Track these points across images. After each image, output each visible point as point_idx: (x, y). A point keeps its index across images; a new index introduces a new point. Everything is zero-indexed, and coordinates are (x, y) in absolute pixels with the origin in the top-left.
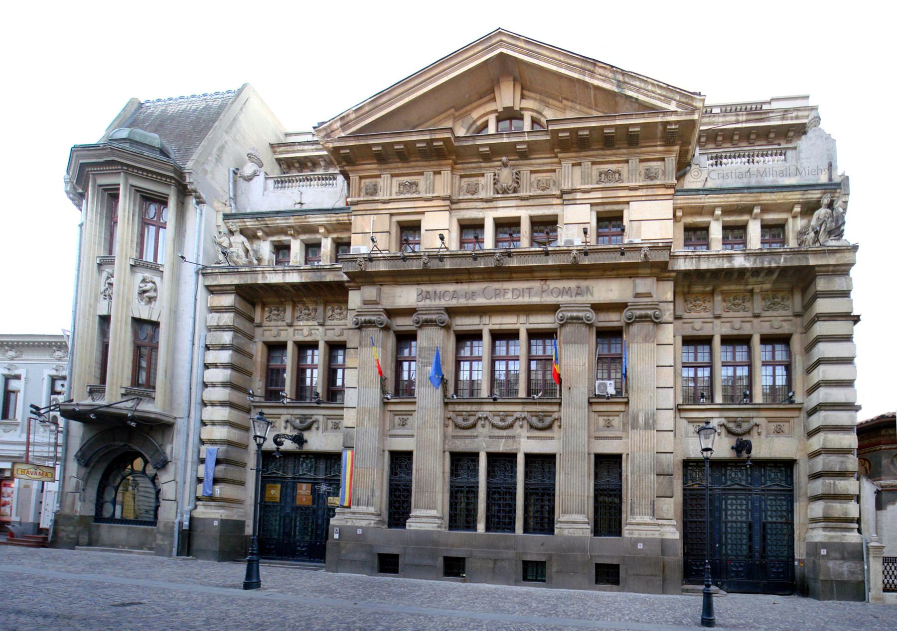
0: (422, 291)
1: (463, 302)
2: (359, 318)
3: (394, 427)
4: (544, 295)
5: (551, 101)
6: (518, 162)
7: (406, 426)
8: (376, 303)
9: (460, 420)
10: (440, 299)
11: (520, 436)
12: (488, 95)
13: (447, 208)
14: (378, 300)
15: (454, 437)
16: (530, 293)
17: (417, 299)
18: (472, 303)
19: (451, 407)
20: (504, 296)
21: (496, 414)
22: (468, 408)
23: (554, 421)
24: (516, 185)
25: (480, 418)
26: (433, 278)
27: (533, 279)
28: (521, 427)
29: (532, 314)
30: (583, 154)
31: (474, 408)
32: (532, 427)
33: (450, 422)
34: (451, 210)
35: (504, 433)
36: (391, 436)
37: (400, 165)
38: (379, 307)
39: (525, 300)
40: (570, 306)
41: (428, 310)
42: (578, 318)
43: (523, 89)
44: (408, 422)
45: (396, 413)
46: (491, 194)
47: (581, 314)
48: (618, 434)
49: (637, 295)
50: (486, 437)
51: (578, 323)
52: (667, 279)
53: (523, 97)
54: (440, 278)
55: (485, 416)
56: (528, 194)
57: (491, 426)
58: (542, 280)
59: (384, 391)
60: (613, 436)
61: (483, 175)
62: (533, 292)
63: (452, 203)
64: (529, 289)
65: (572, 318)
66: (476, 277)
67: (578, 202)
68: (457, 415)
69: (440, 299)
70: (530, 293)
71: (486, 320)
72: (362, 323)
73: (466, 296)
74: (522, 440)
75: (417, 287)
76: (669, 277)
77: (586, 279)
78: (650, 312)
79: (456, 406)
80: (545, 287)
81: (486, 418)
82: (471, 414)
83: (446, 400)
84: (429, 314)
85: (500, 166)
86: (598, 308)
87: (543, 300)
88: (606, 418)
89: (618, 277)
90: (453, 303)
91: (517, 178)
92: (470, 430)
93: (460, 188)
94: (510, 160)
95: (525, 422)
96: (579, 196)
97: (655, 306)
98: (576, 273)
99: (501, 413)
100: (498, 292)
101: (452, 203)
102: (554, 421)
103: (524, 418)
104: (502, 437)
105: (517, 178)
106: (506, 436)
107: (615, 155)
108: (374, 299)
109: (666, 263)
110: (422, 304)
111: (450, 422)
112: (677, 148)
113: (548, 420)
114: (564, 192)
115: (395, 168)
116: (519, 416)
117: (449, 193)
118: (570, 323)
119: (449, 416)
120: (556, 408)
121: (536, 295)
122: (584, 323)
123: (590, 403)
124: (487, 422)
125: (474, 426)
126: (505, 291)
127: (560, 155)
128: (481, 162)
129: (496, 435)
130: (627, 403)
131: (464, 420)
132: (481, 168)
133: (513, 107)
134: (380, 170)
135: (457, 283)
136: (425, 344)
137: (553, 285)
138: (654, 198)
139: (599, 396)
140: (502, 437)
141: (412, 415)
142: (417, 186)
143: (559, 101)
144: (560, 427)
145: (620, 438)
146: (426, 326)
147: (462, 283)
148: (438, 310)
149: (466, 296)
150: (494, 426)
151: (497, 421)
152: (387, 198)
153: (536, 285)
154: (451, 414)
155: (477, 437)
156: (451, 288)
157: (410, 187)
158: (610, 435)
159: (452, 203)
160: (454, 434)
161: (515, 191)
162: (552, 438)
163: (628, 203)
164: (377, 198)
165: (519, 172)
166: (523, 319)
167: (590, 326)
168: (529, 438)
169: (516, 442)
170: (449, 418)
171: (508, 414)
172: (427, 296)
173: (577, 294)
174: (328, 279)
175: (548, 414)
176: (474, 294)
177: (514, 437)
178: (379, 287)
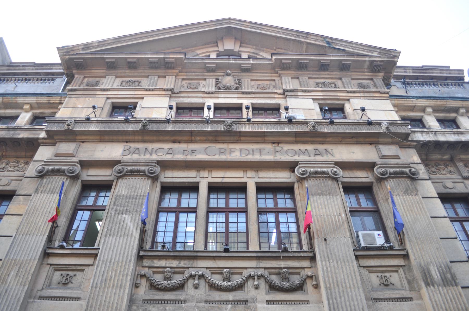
0: (130, 147)
1: (179, 157)
2: (46, 167)
3: (49, 286)
4: (277, 154)
5: (265, 49)
6: (240, 74)
7: (70, 285)
8: (72, 155)
9: (158, 279)
10: (151, 154)
11: (254, 300)
12: (212, 44)
13: (169, 96)
14: (74, 154)
15: (145, 301)
16: (260, 152)
17: (123, 153)
18: (190, 158)
19: (146, 263)
20: (230, 153)
21: (218, 271)
22: (174, 263)
23: (305, 280)
24: (238, 85)
25: (192, 277)
26: (146, 138)
27: (264, 142)
28: (257, 287)
29: (261, 170)
30: (300, 73)
31: (183, 263)
32: (273, 288)
33: (144, 281)
34: (171, 97)
35: (230, 296)
36: (42, 298)
37: (127, 71)
38: (74, 158)
39: (257, 157)
40: (308, 164)
41: (137, 163)
42: (323, 173)
43: (241, 43)
44: (74, 280)
45: (59, 267)
46: (213, 89)
47: (325, 170)
48: (407, 294)
49: (383, 157)
50: (200, 302)
51: (323, 177)
52: (409, 147)
53: (240, 46)
54: (155, 138)
55: (200, 273)
56: (250, 90)
57: (207, 287)
58: (274, 143)
59: (50, 239)
60: (397, 296)
61: (205, 80)
62: (263, 152)
63: (172, 93)
64: (260, 149)
65: (316, 173)
66: (198, 138)
67: (299, 97)
68: (154, 273)
69: (151, 154)
70: (260, 152)
71: (205, 174)
72: (48, 171)
73: (184, 152)
74: (259, 305)
75: (125, 144)
76: (409, 145)
77: (322, 144)
78: (407, 170)
79: (156, 261)
80: (278, 148)
81: (202, 276)
82: (176, 271)
83: (142, 253)
84: (136, 165)
85: (223, 75)
86: (344, 165)
87: (276, 158)
88: (380, 274)
89: (357, 143)
90: (169, 157)
91: (238, 82)
92: (174, 293)
93: (182, 86)
94: (232, 72)
95: (262, 283)
96: (300, 94)
97: (407, 165)
98: (312, 139)
99: (225, 270)
100: (222, 151)
101: (172, 93)
102: (305, 280)
103: (262, 276)
104: (227, 302)
105: (238, 82)
106: (232, 301)
107: (329, 74)
108: (71, 152)
109: (408, 135)
110: (128, 157)
111: (144, 281)
112: (382, 74)
113: (296, 280)
114: (285, 91)
115: (121, 73)
116: (252, 273)
117: (172, 87)
118: (313, 177)
119: (143, 273)
120: (306, 264)
121: (268, 153)
122: (330, 177)
123: (357, 257)
124: (202, 282)
125: (181, 286)
126: (232, 151)
127: (280, 72)
128: (205, 72)
129: (217, 298)
130: (406, 256)
131: (166, 279)
132: (204, 75)
133: (233, 50)
134: (106, 73)
135: (174, 142)
136: (124, 192)
137: (286, 147)
138: (371, 98)
139: (367, 249)
140: (227, 302)
141: (83, 270)
142: (140, 83)
143: (273, 49)
144: (317, 287)
145: (410, 299)
146: (130, 176)
147: (179, 142)
148: (148, 163)
149: (184, 152)
150: (213, 287)
151: (217, 280)
152: (109, 87)
153: (268, 147)
154: (145, 271)
155: (185, 301)
156: (166, 146)
157: (132, 83)
158: (394, 296)
159: (172, 93)
160: (148, 298)
161: (237, 88)
162: (307, 302)
163: (348, 100)
164: (98, 88)
165: (241, 79)
166: (250, 174)
167: (336, 180)
168: (268, 302)
169: (249, 308)
170: (142, 276)
171: (234, 272)
172: (137, 151)
173: (316, 154)
174: (21, 136)
175: (295, 271)
176: (193, 151)
177: (246, 302)
178: (78, 143)
